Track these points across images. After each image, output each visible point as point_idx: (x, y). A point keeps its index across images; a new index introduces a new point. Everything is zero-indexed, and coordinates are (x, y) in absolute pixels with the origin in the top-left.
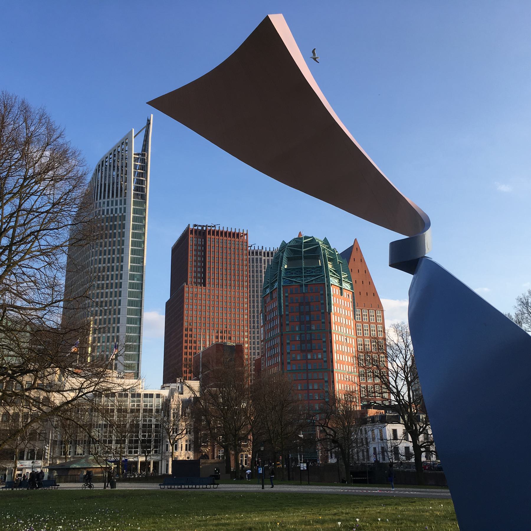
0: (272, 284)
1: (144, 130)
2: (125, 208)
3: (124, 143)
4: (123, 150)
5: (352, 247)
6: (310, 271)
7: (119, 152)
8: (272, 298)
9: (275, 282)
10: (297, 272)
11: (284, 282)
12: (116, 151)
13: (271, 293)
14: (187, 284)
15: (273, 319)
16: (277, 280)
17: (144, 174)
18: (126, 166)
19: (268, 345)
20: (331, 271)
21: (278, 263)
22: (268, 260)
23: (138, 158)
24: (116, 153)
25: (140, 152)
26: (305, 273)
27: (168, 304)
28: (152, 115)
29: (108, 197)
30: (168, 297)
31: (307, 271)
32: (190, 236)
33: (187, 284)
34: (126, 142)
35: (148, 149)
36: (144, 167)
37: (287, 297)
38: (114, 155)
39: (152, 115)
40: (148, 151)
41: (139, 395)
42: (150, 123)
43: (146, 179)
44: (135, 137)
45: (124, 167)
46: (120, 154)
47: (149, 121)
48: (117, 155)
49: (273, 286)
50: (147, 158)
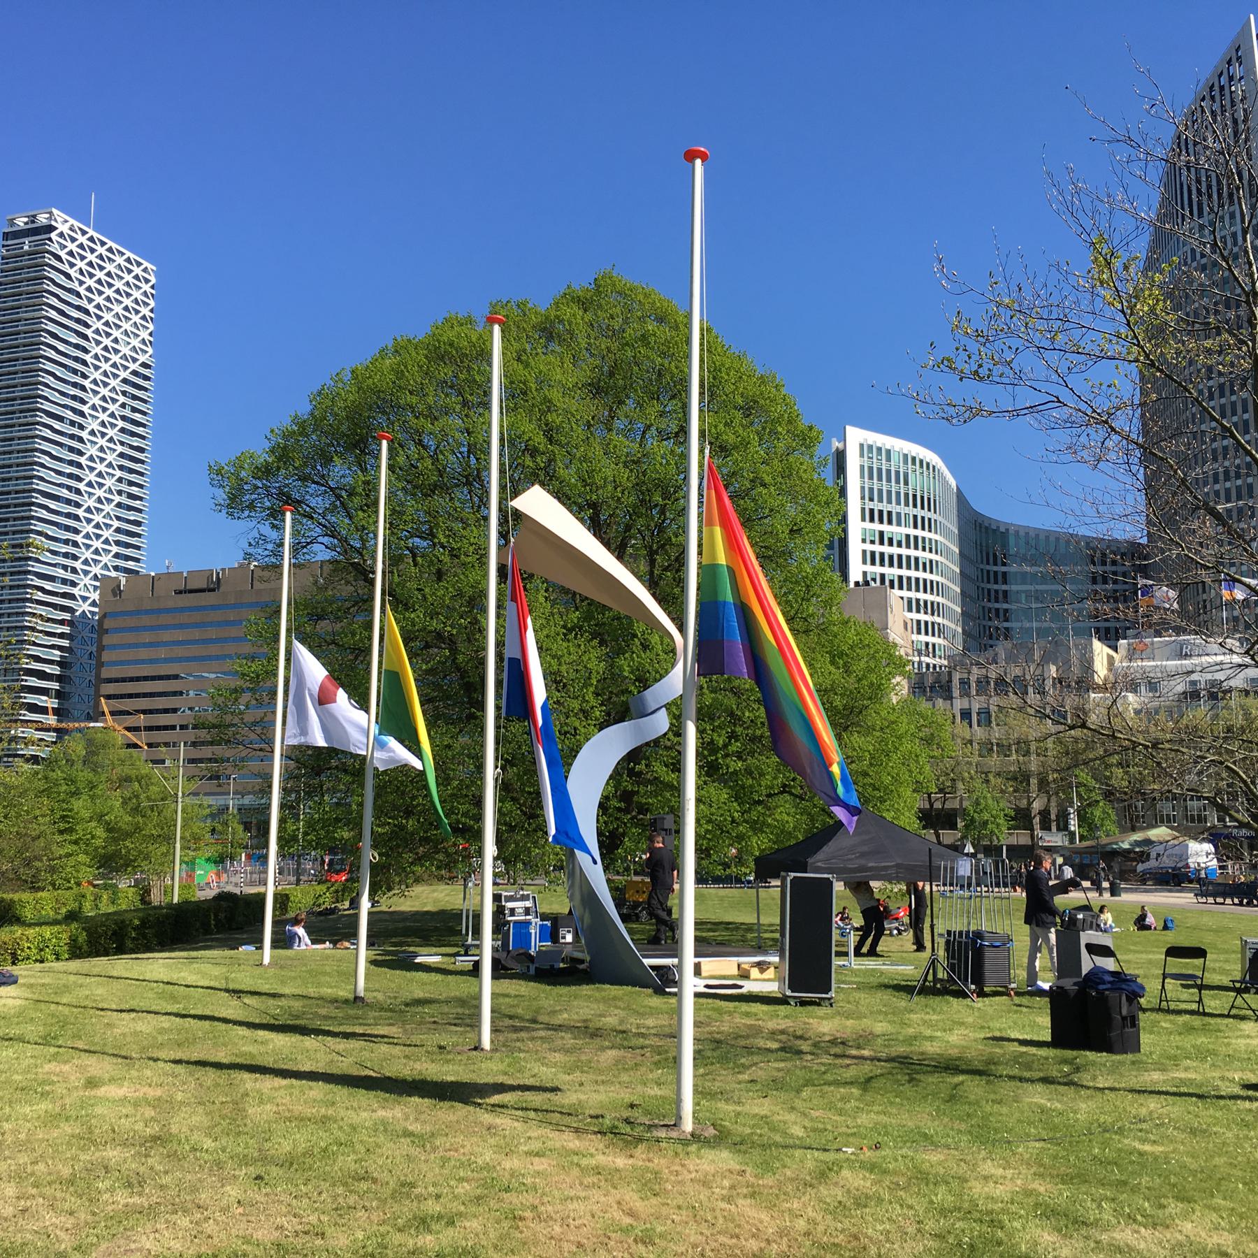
3: (1234, 59)
4: (1231, 78)
7: (1222, 88)
12: (1216, 88)
24: (1216, 93)
38: (1213, 98)
48: (1218, 98)
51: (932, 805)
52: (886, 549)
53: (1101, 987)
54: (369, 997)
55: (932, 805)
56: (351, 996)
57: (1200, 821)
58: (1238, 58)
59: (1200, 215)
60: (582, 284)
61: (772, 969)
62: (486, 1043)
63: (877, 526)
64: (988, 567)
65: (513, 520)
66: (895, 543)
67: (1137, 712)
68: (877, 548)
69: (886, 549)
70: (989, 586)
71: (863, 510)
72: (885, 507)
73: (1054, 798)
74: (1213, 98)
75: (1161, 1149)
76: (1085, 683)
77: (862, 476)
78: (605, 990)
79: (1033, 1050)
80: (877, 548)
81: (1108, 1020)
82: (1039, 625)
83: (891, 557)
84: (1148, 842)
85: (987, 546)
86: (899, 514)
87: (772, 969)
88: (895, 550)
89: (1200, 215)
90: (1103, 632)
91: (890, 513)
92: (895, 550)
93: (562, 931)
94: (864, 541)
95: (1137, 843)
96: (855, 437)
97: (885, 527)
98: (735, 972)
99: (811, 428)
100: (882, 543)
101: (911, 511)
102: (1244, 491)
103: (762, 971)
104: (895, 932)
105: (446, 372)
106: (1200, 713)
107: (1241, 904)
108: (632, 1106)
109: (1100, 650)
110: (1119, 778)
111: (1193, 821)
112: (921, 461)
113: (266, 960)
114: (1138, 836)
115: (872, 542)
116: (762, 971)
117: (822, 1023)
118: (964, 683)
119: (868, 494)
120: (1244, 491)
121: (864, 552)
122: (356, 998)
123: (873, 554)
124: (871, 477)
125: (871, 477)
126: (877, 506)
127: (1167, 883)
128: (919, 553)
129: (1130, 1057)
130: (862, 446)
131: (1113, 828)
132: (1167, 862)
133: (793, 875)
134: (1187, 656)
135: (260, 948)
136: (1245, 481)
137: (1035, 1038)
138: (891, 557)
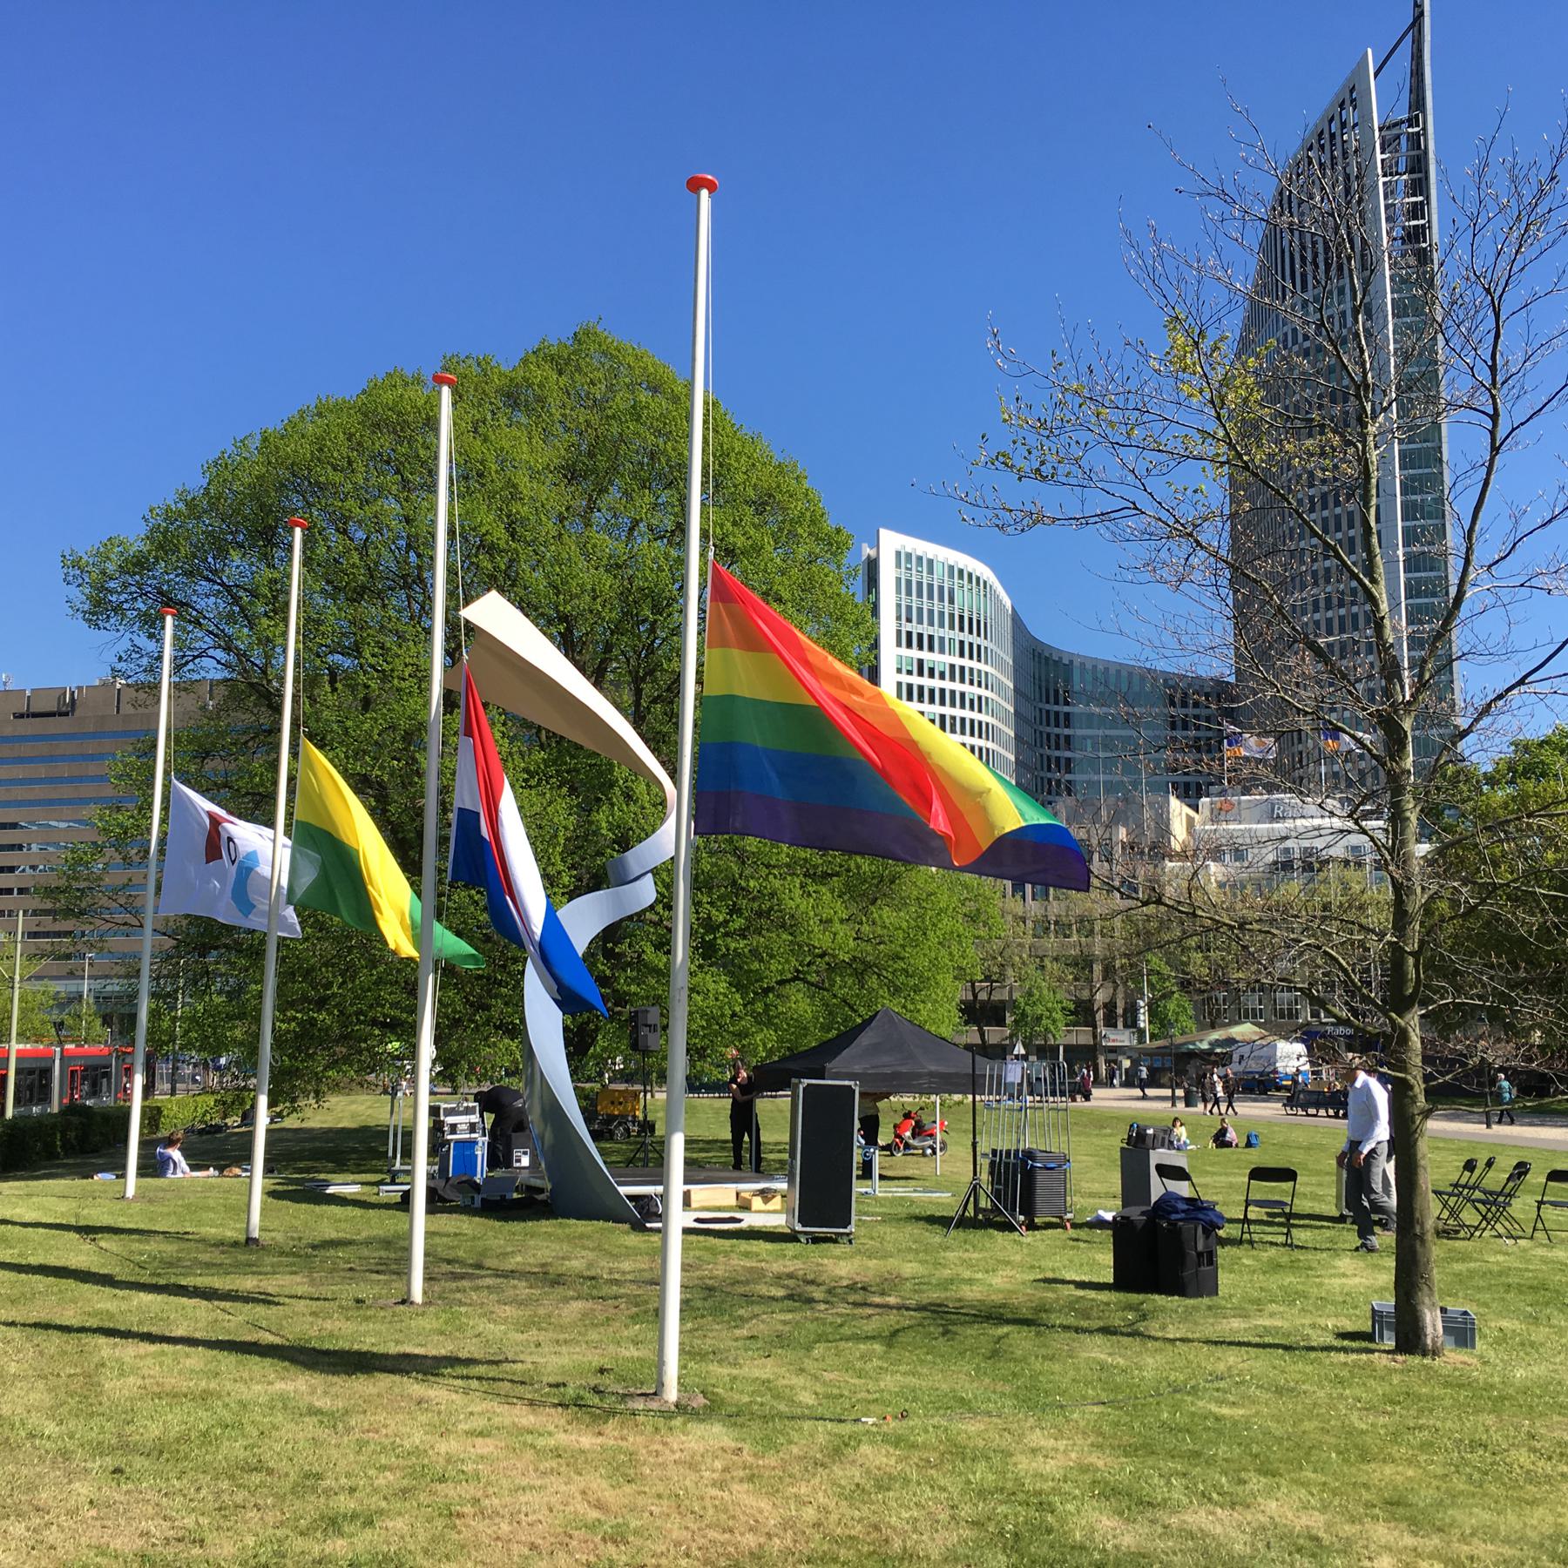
1: (1409, 37)
3: (1348, 102)
4: (1343, 125)
7: (1333, 136)
12: (1326, 135)
17: (1419, 186)
24: (1326, 141)
34: (1352, 97)
35: (1424, 99)
36: (1418, 165)
38: (1322, 147)
40: (1424, 105)
42: (1422, 14)
43: (1428, 198)
44: (1376, 75)
45: (1352, 178)
46: (1338, 140)
48: (1327, 147)
50: (1424, 129)
51: (975, 996)
52: (926, 682)
53: (1174, 1216)
54: (266, 1238)
55: (975, 996)
56: (242, 1238)
57: (1290, 1016)
58: (1353, 100)
59: (1304, 288)
60: (558, 335)
61: (778, 1199)
62: (417, 1295)
63: (915, 653)
64: (1048, 707)
65: (461, 634)
67: (1221, 885)
68: (915, 680)
69: (926, 682)
70: (1048, 729)
71: (899, 632)
72: (926, 630)
73: (1121, 988)
74: (1322, 147)
75: (1241, 1412)
76: (1159, 850)
77: (898, 591)
78: (569, 1226)
79: (1092, 1294)
80: (915, 680)
81: (1179, 1256)
82: (1109, 777)
83: (932, 692)
84: (1231, 1041)
85: (1047, 681)
86: (942, 639)
87: (778, 1199)
88: (936, 683)
89: (1304, 288)
90: (1181, 790)
91: (931, 638)
92: (936, 683)
93: (516, 1153)
94: (899, 671)
95: (1217, 1043)
96: (891, 542)
97: (925, 655)
98: (733, 1202)
99: (838, 531)
100: (921, 673)
101: (957, 635)
102: (1348, 623)
103: (766, 1200)
104: (929, 1151)
105: (384, 442)
106: (1292, 888)
107: (1336, 1116)
108: (602, 1371)
109: (1178, 809)
110: (1198, 965)
111: (1282, 1017)
112: (970, 575)
113: (130, 1192)
114: (1216, 1035)
115: (910, 673)
116: (766, 1200)
117: (839, 1264)
119: (905, 614)
120: (1348, 623)
121: (899, 684)
122: (250, 1241)
123: (910, 686)
124: (909, 593)
125: (909, 593)
126: (915, 628)
127: (1252, 1091)
128: (966, 688)
129: (1206, 1301)
130: (898, 554)
131: (1190, 1024)
132: (1253, 1066)
133: (806, 1082)
134: (1279, 818)
135: (123, 1176)
136: (1349, 611)
137: (1095, 1280)
138: (932, 692)
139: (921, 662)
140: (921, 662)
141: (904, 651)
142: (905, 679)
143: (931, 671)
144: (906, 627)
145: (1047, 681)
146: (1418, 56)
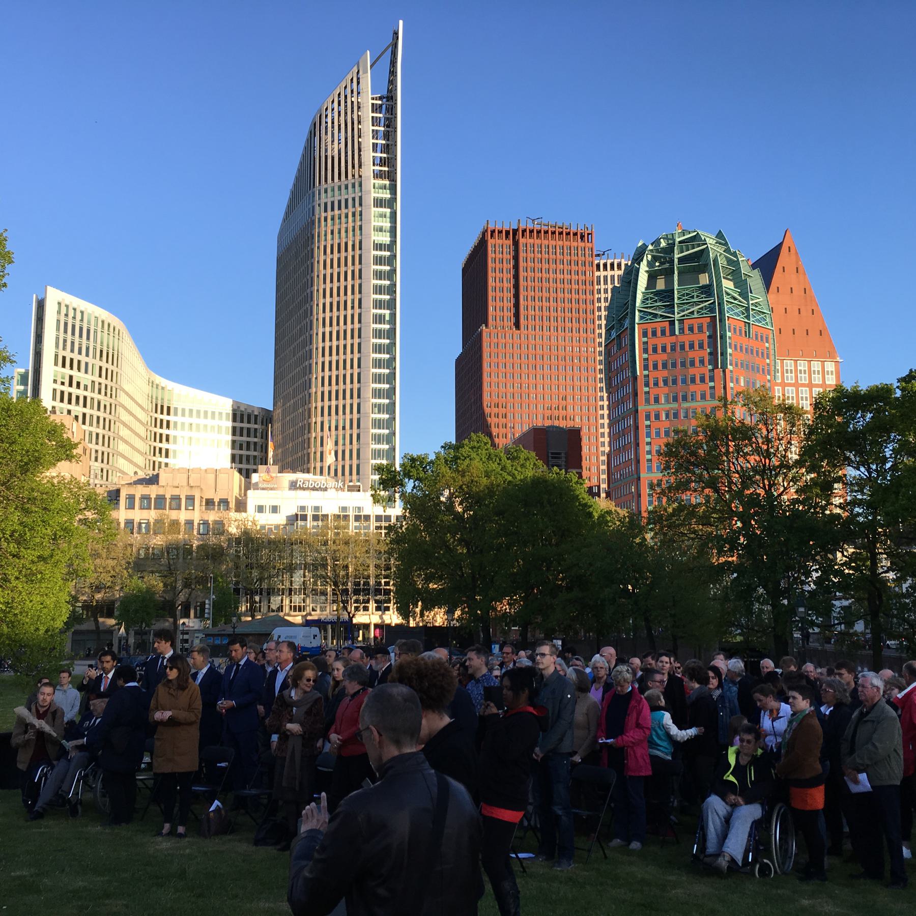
0: (621, 321)
2: (361, 198)
5: (779, 248)
6: (688, 294)
8: (620, 347)
9: (624, 318)
10: (664, 297)
11: (641, 318)
13: (619, 336)
14: (487, 326)
15: (623, 384)
16: (627, 314)
18: (359, 122)
19: (616, 429)
20: (728, 294)
21: (630, 282)
22: (613, 277)
23: (381, 106)
25: (385, 93)
26: (679, 298)
27: (459, 362)
28: (401, 22)
29: (333, 179)
30: (459, 350)
31: (683, 295)
32: (491, 242)
33: (487, 326)
37: (644, 343)
39: (401, 22)
41: (367, 518)
44: (371, 66)
47: (396, 34)
49: (622, 325)
52: (74, 391)
63: (67, 371)
66: (82, 386)
68: (66, 389)
69: (74, 391)
71: (56, 356)
72: (76, 357)
75: (261, 905)
77: (58, 329)
80: (66, 389)
83: (78, 398)
85: (157, 398)
88: (81, 392)
94: (55, 381)
100: (71, 385)
112: (109, 325)
115: (63, 383)
118: (131, 498)
121: (55, 390)
130: (59, 304)
138: (78, 398)
139: (71, 377)
140: (71, 377)
141: (59, 368)
142: (60, 388)
143: (78, 384)
144: (61, 353)
145: (157, 398)
146: (393, 63)
